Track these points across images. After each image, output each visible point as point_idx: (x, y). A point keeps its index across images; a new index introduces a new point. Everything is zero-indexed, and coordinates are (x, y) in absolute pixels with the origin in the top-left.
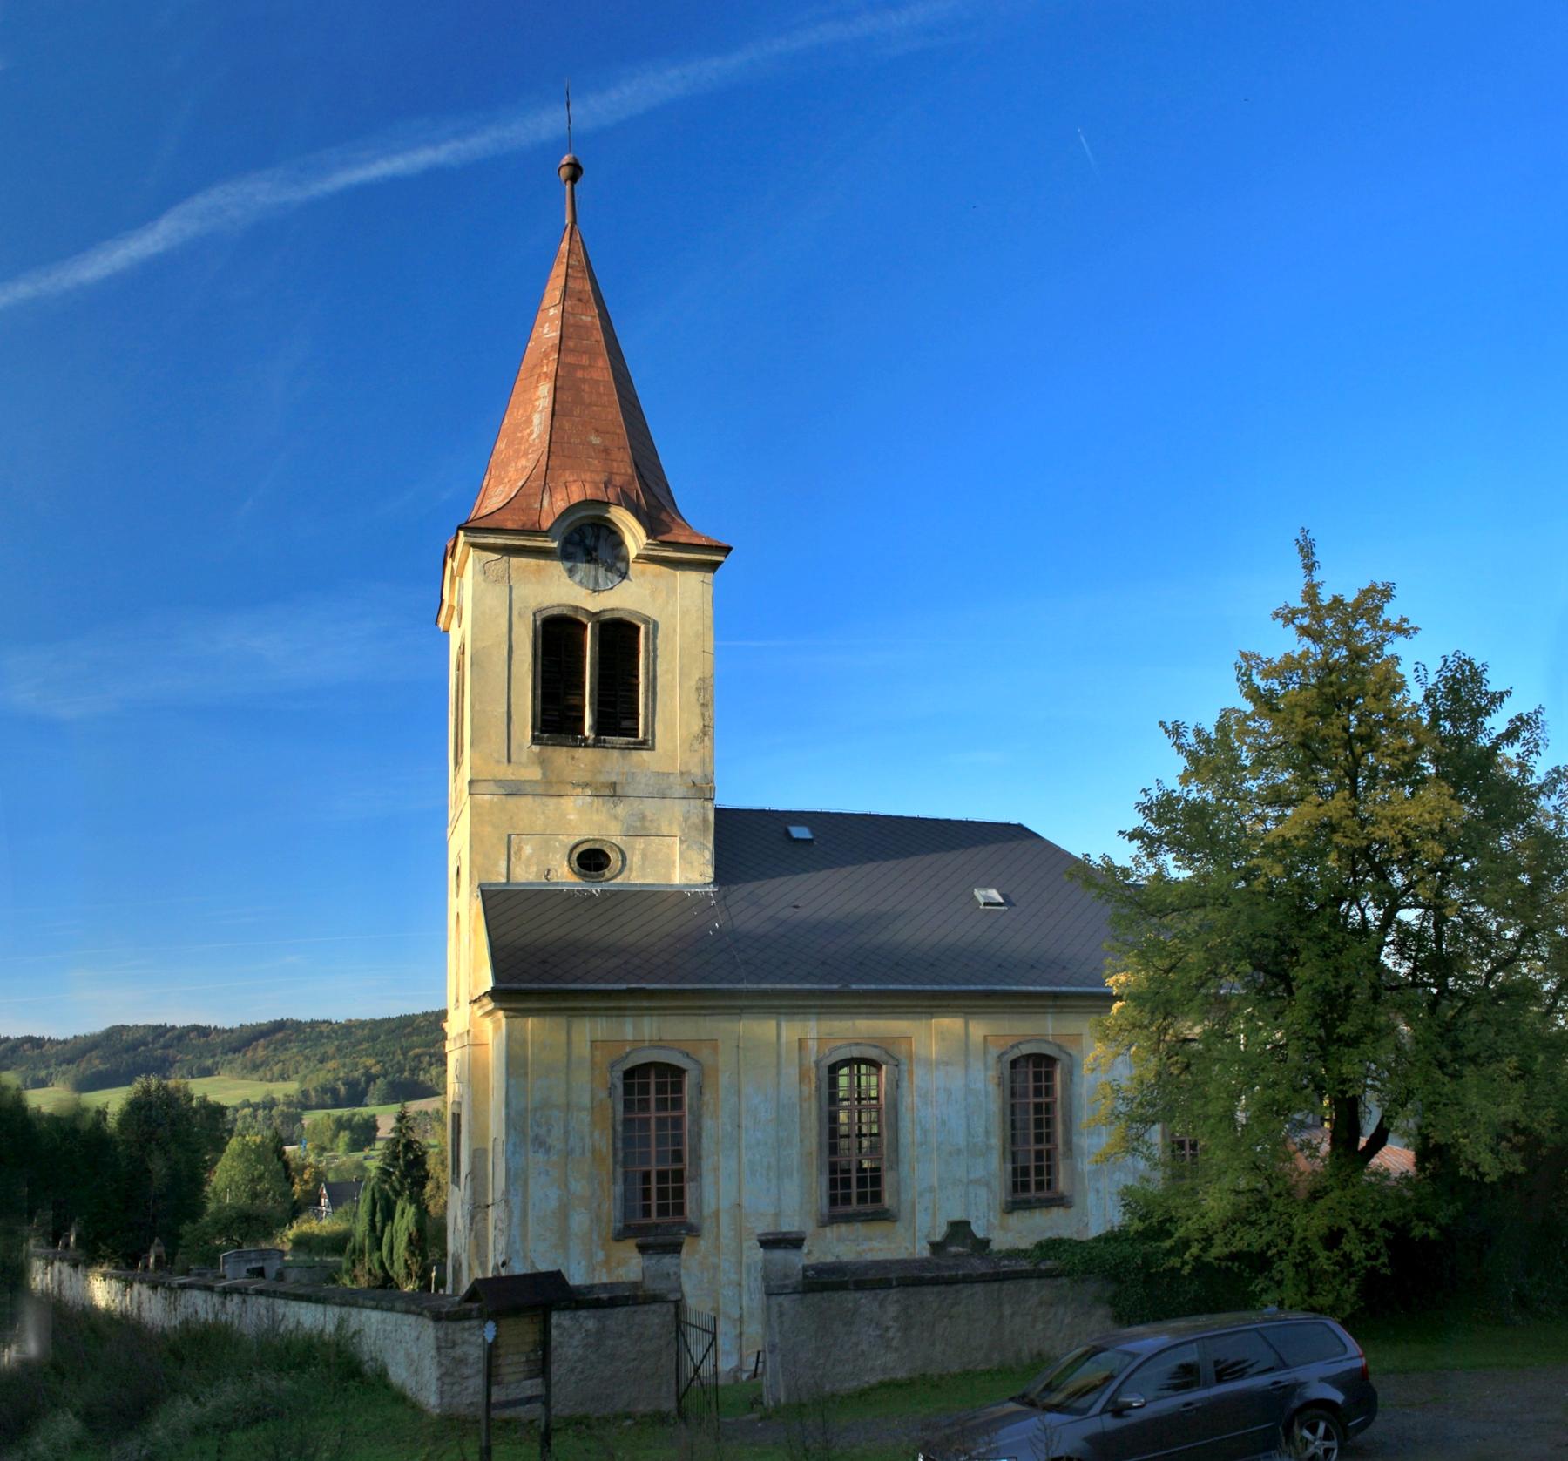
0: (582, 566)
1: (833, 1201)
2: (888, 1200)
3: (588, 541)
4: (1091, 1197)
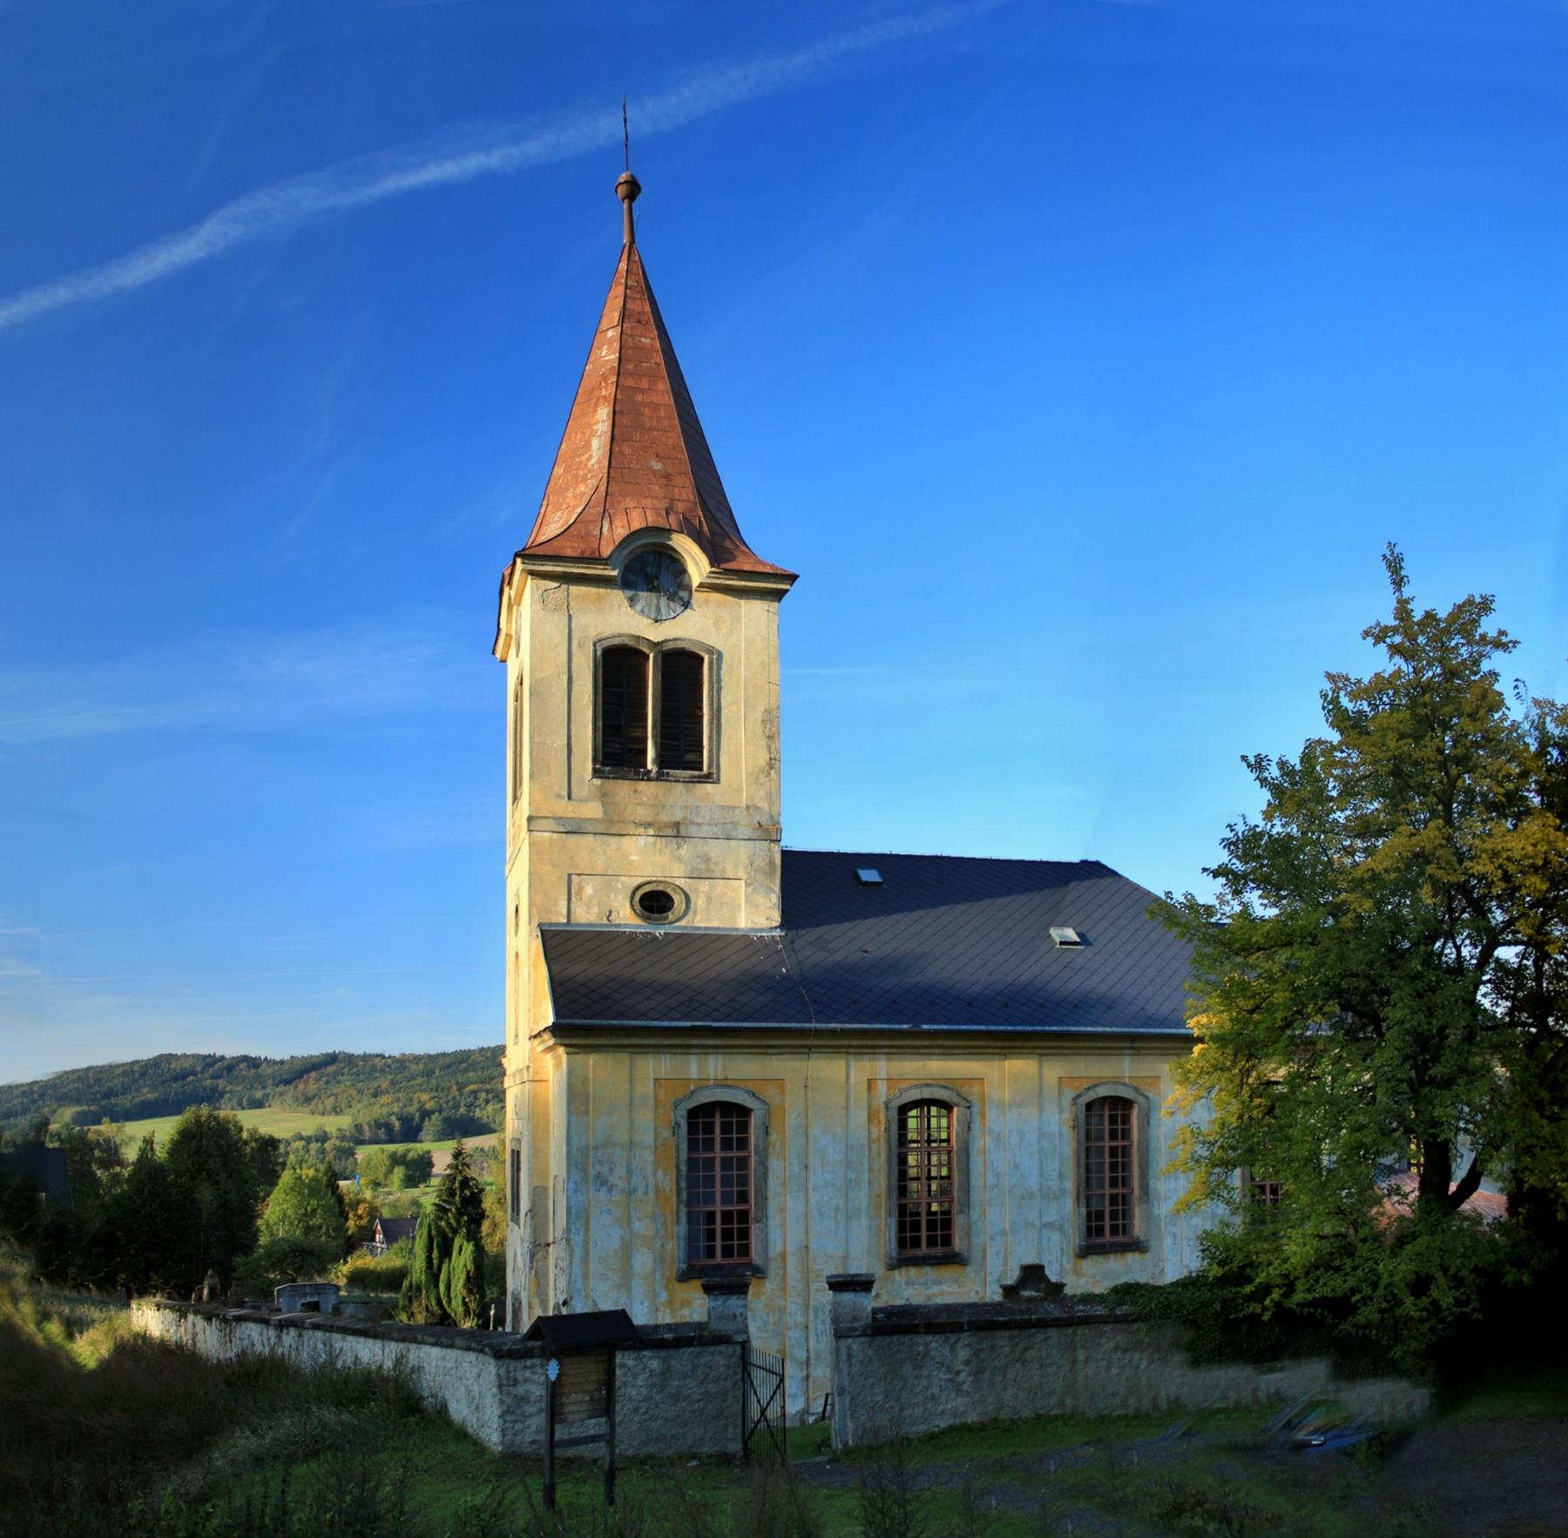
0: (643, 595)
1: (902, 1243)
2: (958, 1244)
3: (648, 569)
4: (1168, 1242)
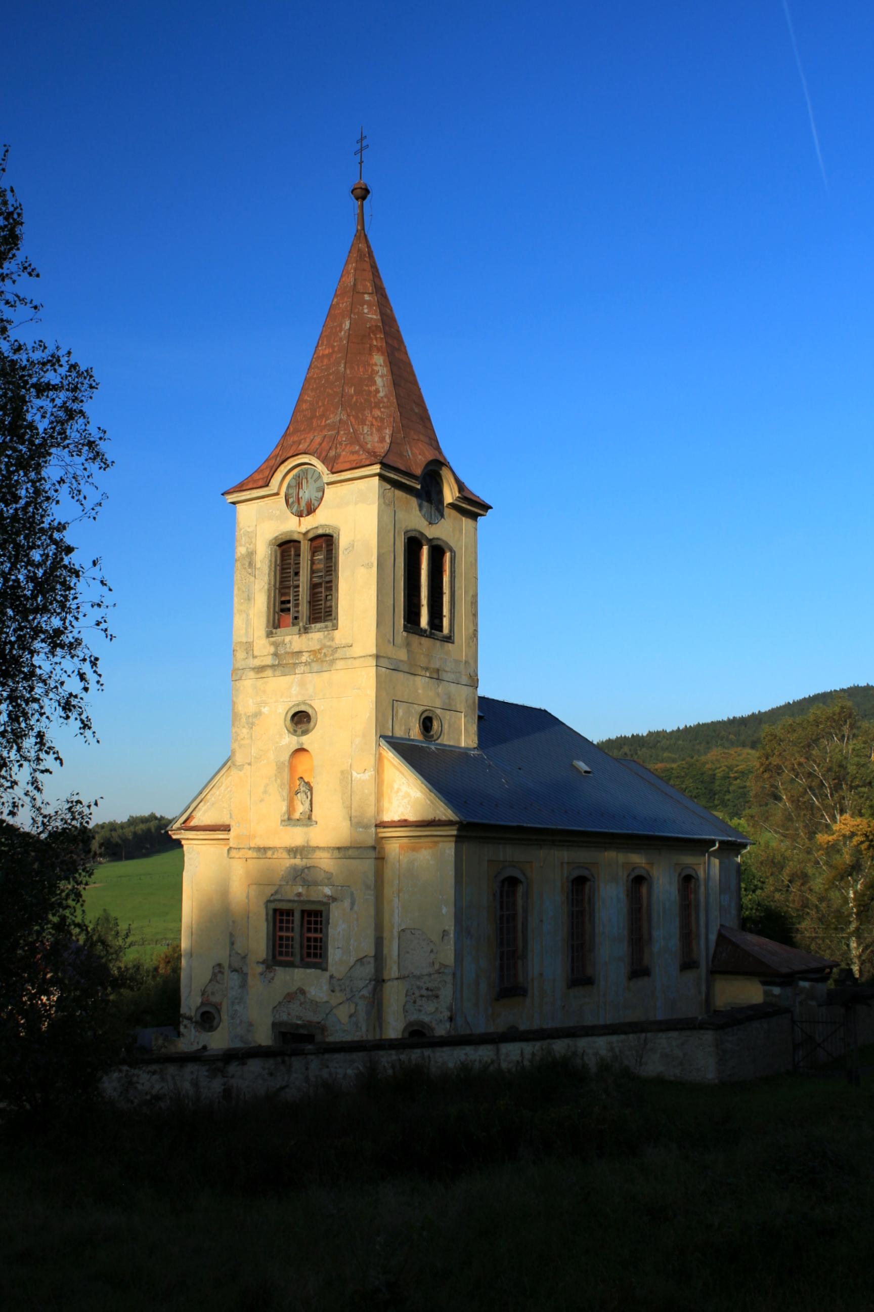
0: (425, 504)
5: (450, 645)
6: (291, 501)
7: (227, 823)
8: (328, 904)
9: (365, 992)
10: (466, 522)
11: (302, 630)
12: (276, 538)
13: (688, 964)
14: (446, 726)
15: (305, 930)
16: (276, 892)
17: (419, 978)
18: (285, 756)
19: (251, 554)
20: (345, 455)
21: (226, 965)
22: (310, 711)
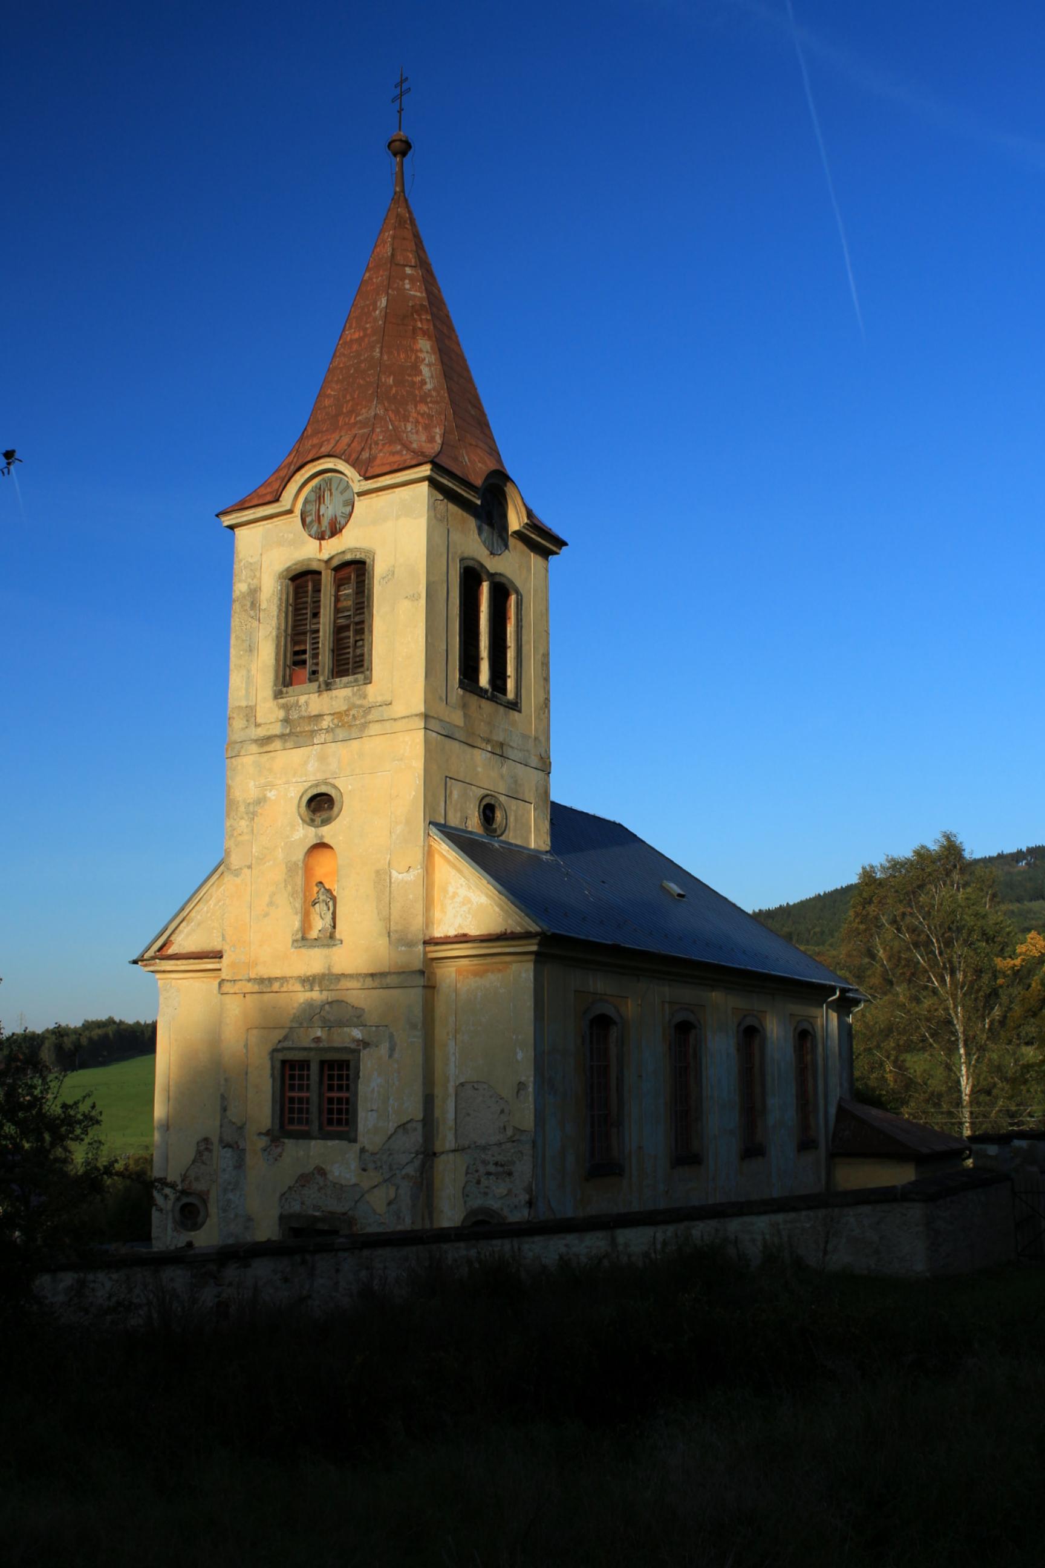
0: (486, 527)
5: (516, 713)
6: (308, 520)
7: (218, 948)
8: (359, 1051)
9: (410, 1170)
10: (535, 559)
11: (323, 686)
12: (288, 569)
13: (806, 1144)
14: (512, 819)
15: (325, 1087)
16: (286, 1038)
17: (484, 1148)
18: (299, 855)
19: (254, 592)
20: (384, 457)
21: (215, 1140)
22: (333, 793)
